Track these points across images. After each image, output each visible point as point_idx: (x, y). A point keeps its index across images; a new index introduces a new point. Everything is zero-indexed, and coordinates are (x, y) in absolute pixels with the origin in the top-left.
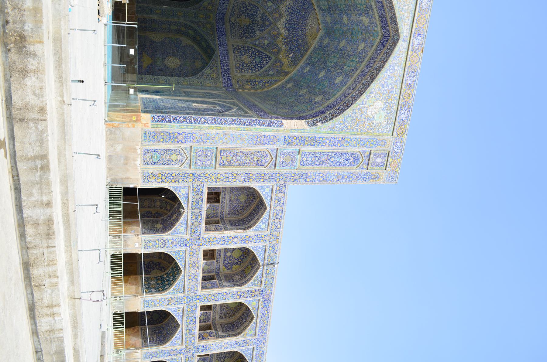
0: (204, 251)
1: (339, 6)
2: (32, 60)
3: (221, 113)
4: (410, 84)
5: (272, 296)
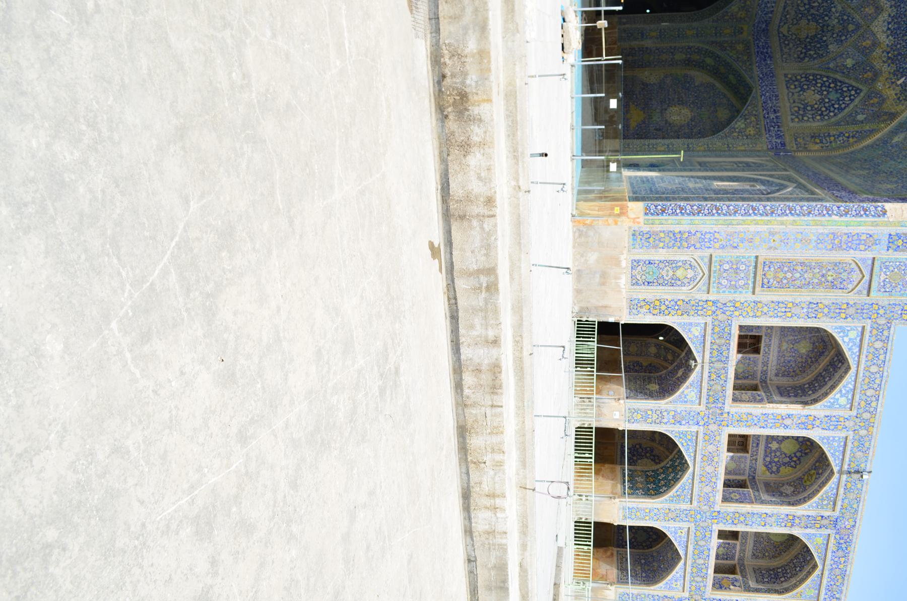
0: (730, 436)
2: (476, 128)
3: (765, 196)
5: (855, 532)
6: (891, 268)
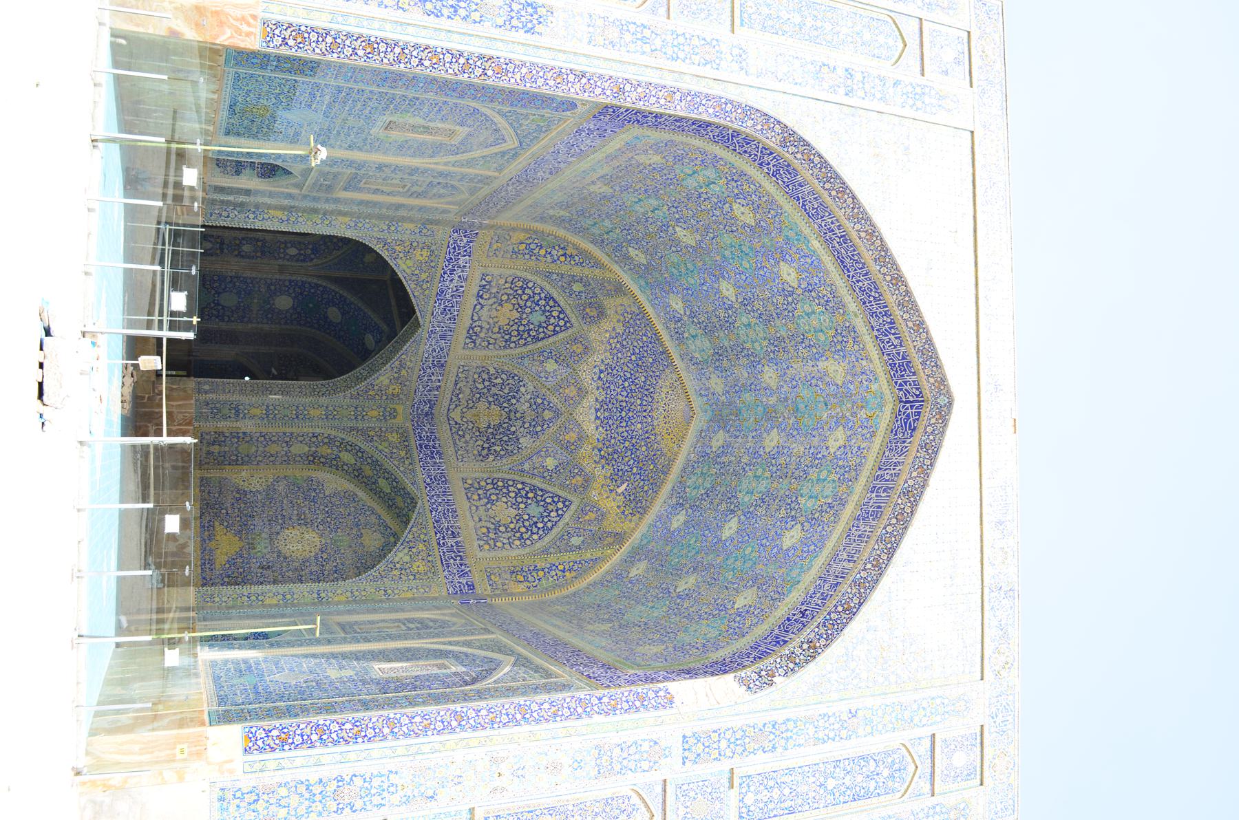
1: (748, 345)
4: (1001, 523)
6: (692, 794)
